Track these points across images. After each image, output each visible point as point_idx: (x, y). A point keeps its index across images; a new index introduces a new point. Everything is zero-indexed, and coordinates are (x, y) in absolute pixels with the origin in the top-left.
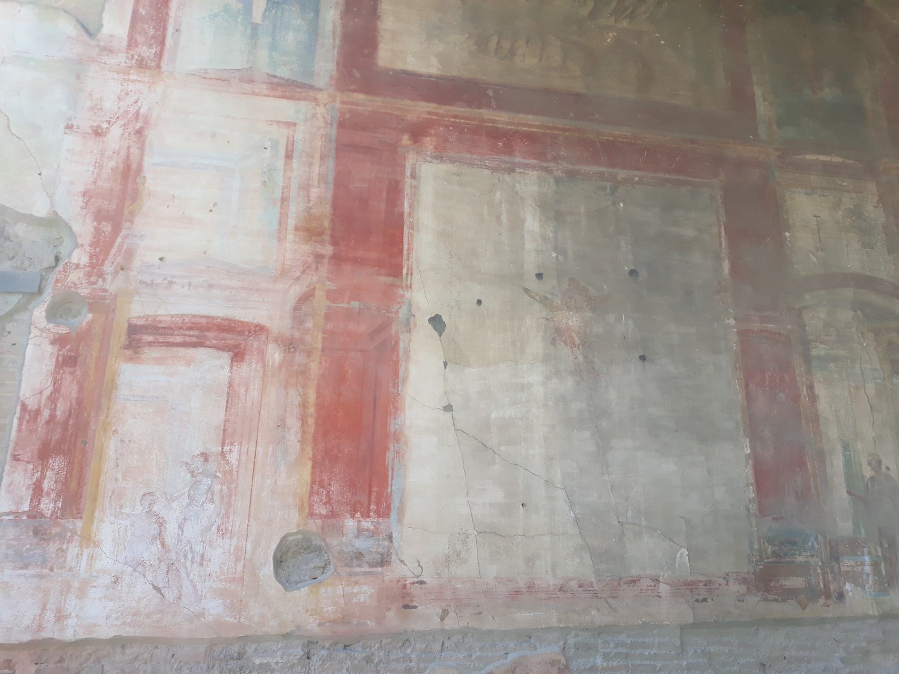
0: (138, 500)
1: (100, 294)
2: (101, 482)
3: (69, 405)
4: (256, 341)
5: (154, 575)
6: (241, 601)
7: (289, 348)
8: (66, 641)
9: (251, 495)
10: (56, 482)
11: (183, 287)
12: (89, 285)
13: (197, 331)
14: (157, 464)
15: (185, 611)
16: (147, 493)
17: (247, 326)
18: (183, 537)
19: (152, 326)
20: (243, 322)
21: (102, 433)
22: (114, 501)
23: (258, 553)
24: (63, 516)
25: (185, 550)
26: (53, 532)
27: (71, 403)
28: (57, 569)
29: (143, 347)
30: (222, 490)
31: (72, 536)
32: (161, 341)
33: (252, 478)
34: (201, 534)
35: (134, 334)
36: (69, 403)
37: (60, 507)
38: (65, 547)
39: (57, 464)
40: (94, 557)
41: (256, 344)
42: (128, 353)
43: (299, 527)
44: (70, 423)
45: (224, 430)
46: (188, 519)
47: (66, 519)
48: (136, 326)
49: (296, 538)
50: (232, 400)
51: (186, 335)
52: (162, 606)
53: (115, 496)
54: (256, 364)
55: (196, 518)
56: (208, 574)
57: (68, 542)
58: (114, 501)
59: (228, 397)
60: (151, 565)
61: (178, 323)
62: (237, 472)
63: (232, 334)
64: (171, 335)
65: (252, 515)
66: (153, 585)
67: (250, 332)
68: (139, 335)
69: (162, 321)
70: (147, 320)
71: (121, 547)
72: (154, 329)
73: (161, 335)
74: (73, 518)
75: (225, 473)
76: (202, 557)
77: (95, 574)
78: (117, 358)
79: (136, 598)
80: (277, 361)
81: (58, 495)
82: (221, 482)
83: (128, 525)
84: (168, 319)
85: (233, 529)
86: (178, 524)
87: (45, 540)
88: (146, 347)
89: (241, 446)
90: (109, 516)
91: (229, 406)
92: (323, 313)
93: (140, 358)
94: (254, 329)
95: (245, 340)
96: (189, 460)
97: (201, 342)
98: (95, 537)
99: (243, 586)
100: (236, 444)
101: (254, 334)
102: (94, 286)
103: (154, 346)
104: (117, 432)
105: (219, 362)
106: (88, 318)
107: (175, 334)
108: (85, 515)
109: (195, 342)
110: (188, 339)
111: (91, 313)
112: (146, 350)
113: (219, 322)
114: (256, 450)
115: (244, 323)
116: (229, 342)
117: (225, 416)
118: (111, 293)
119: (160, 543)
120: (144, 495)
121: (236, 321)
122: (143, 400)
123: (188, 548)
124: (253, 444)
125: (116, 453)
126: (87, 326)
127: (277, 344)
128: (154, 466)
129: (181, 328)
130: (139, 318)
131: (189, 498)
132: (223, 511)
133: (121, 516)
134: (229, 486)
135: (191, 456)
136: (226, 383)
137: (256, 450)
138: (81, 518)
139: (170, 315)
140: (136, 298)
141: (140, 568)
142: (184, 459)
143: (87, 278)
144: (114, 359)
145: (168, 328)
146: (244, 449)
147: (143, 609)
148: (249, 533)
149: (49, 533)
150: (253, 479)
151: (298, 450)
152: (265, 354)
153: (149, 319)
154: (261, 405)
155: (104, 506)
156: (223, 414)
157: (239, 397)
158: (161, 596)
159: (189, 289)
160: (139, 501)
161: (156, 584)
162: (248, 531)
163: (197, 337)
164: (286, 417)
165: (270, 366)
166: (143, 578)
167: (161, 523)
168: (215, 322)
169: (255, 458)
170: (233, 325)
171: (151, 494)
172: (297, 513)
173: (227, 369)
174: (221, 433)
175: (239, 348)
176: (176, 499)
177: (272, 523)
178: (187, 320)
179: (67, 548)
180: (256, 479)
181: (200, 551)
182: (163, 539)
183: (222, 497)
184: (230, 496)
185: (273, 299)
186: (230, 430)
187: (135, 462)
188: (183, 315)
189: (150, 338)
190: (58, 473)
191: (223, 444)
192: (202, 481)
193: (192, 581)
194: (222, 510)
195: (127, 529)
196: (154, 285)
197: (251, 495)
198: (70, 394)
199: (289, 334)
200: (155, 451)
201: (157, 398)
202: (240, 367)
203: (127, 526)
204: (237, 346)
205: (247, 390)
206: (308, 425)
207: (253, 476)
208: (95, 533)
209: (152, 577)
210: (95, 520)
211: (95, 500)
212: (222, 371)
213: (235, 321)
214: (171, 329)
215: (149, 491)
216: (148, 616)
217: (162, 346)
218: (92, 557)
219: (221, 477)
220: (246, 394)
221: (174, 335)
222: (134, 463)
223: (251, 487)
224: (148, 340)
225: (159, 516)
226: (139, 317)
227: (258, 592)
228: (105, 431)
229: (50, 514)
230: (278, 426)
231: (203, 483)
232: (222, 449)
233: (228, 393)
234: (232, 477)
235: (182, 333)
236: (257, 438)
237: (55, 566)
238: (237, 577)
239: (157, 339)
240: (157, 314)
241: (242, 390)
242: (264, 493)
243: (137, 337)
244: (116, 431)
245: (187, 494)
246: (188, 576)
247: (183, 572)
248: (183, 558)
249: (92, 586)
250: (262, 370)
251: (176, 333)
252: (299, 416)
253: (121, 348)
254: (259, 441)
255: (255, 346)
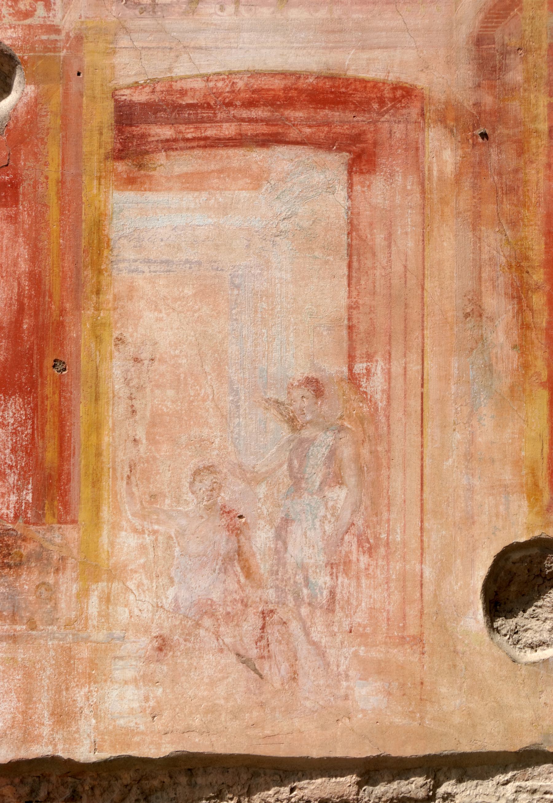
0: (186, 484)
1: (44, 37)
2: (104, 447)
3: (16, 290)
4: (399, 122)
5: (236, 633)
6: (422, 683)
7: (473, 135)
8: (81, 761)
9: (422, 466)
10: (14, 451)
11: (222, 9)
12: (20, 20)
13: (266, 109)
14: (216, 406)
15: (308, 704)
16: (202, 466)
17: (376, 90)
18: (288, 555)
19: (167, 105)
20: (363, 81)
21: (93, 345)
22: (137, 485)
23: (448, 587)
24: (39, 520)
25: (295, 582)
26: (24, 552)
27: (19, 284)
28: (42, 625)
29: (153, 152)
30: (357, 457)
31: (63, 559)
32: (189, 136)
33: (419, 429)
34: (324, 549)
35: (131, 125)
36: (16, 284)
37: (31, 501)
38: (51, 580)
39: (11, 414)
40: (112, 598)
41: (399, 130)
42: (121, 167)
43: (533, 532)
44: (25, 326)
45: (350, 328)
46: (293, 521)
47: (44, 524)
48: (131, 105)
49: (528, 554)
50: (359, 261)
51: (243, 120)
52: (261, 694)
53: (138, 476)
54: (405, 176)
55: (309, 517)
56: (348, 629)
57: (57, 570)
58: (137, 485)
59: (350, 256)
60: (228, 613)
61: (221, 94)
62: (388, 417)
63: (344, 110)
64: (211, 120)
65: (428, 506)
66: (238, 655)
67: (382, 102)
68: (143, 126)
69: (186, 91)
70: (153, 92)
71: (163, 580)
72: (173, 111)
73: (188, 122)
74: (59, 522)
75: (361, 420)
76: (332, 594)
77: (118, 632)
78: (103, 181)
79: (206, 680)
80: (450, 169)
81: (23, 476)
82: (355, 439)
83: (173, 535)
84: (199, 84)
85: (391, 537)
86: (273, 530)
87: (10, 567)
88: (160, 151)
89: (390, 362)
90: (130, 517)
91: (354, 274)
92: (545, 46)
93: (149, 176)
94: (391, 96)
95: (375, 122)
96: (283, 398)
97: (278, 134)
98: (108, 559)
99: (423, 654)
100: (378, 357)
101: (393, 106)
102: (28, 21)
103: (176, 149)
104: (123, 342)
105: (322, 177)
106: (27, 94)
107: (218, 118)
108: (83, 515)
109: (263, 134)
110: (248, 129)
111: (30, 84)
112: (161, 158)
113: (312, 84)
114: (423, 368)
115: (368, 82)
116: (338, 130)
117: (349, 297)
118: (68, 34)
119: (242, 568)
120: (197, 473)
121: (348, 80)
122: (169, 271)
123: (300, 578)
124: (414, 357)
125: (128, 384)
126: (28, 113)
127: (446, 127)
128: (211, 410)
129: (229, 104)
130: (136, 88)
131: (290, 476)
132: (367, 501)
133: (156, 517)
134: (373, 448)
135: (286, 386)
136: (343, 222)
137: (423, 368)
138: (74, 522)
139: (202, 76)
140: (124, 42)
141: (207, 622)
142: (271, 394)
143: (10, 3)
144: (95, 182)
145: (202, 107)
146: (397, 368)
147: (222, 702)
148: (426, 545)
149: (16, 553)
150: (422, 431)
151: (515, 366)
152: (420, 153)
153: (158, 88)
154: (424, 268)
155: (119, 497)
156: (343, 292)
157: (374, 254)
158: (257, 676)
159: (237, 13)
160: (188, 485)
161: (242, 652)
162: (422, 541)
163: (267, 122)
164: (481, 292)
165: (435, 179)
166: (216, 641)
167: (238, 529)
168: (302, 84)
169: (422, 386)
170: (343, 90)
171: (210, 469)
172: (525, 503)
173: (342, 193)
174: (345, 333)
175: (361, 142)
176: (264, 479)
177: (473, 523)
178: (240, 84)
179: (56, 583)
180: (428, 431)
181: (325, 583)
182: (247, 560)
183: (360, 470)
184: (378, 468)
185: (427, 21)
186: (362, 327)
187: (169, 404)
188: (230, 73)
189: (167, 132)
190: (15, 433)
191: (351, 358)
192: (315, 439)
193: (314, 644)
194: (364, 498)
195: (171, 542)
196: (157, 9)
197: (422, 466)
198: (15, 264)
199: (471, 103)
200: (209, 377)
201: (199, 263)
202: (369, 186)
203: (170, 537)
204: (357, 138)
205: (389, 238)
206: (531, 310)
207: (422, 427)
208: (108, 552)
209: (234, 637)
210: (105, 526)
211: (96, 483)
212: (331, 196)
213: (348, 82)
214: (209, 106)
215: (207, 464)
216: (235, 715)
217: (193, 148)
218: (108, 600)
219: (354, 429)
220: (389, 246)
221: (217, 122)
222: (167, 408)
223: (420, 449)
224: (162, 137)
225: (232, 515)
226: (136, 86)
227: (455, 666)
228: (98, 339)
229: (12, 515)
230: (467, 315)
231: (317, 442)
232: (350, 369)
233: (350, 246)
234: (377, 429)
235: (234, 117)
236: (423, 343)
237: (37, 618)
238: (409, 636)
239: (180, 132)
240: (173, 75)
241: (379, 239)
242: (450, 460)
243: (137, 130)
244: (120, 340)
245: (285, 467)
246: (307, 634)
247: (295, 627)
248: (292, 600)
249: (115, 658)
250: (417, 189)
251: (220, 115)
252: (510, 291)
253: (106, 158)
254: (427, 348)
255: (398, 135)
